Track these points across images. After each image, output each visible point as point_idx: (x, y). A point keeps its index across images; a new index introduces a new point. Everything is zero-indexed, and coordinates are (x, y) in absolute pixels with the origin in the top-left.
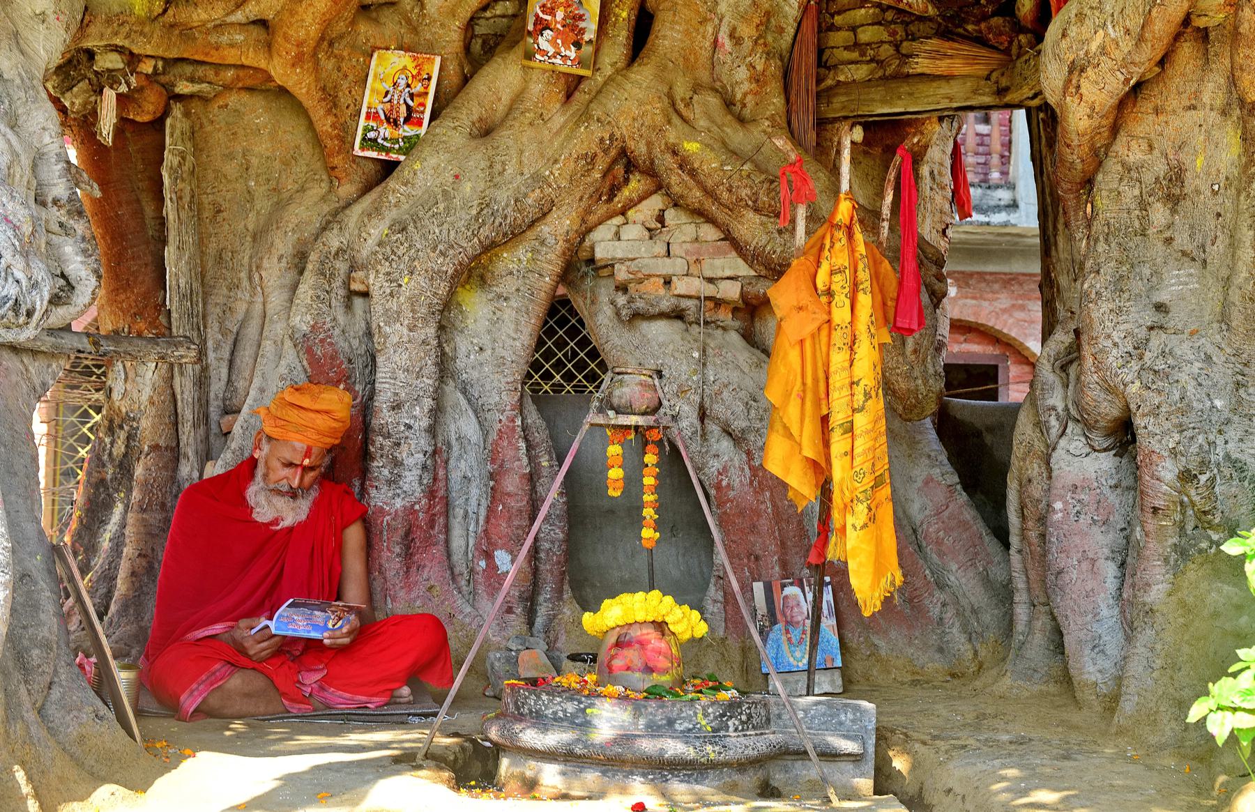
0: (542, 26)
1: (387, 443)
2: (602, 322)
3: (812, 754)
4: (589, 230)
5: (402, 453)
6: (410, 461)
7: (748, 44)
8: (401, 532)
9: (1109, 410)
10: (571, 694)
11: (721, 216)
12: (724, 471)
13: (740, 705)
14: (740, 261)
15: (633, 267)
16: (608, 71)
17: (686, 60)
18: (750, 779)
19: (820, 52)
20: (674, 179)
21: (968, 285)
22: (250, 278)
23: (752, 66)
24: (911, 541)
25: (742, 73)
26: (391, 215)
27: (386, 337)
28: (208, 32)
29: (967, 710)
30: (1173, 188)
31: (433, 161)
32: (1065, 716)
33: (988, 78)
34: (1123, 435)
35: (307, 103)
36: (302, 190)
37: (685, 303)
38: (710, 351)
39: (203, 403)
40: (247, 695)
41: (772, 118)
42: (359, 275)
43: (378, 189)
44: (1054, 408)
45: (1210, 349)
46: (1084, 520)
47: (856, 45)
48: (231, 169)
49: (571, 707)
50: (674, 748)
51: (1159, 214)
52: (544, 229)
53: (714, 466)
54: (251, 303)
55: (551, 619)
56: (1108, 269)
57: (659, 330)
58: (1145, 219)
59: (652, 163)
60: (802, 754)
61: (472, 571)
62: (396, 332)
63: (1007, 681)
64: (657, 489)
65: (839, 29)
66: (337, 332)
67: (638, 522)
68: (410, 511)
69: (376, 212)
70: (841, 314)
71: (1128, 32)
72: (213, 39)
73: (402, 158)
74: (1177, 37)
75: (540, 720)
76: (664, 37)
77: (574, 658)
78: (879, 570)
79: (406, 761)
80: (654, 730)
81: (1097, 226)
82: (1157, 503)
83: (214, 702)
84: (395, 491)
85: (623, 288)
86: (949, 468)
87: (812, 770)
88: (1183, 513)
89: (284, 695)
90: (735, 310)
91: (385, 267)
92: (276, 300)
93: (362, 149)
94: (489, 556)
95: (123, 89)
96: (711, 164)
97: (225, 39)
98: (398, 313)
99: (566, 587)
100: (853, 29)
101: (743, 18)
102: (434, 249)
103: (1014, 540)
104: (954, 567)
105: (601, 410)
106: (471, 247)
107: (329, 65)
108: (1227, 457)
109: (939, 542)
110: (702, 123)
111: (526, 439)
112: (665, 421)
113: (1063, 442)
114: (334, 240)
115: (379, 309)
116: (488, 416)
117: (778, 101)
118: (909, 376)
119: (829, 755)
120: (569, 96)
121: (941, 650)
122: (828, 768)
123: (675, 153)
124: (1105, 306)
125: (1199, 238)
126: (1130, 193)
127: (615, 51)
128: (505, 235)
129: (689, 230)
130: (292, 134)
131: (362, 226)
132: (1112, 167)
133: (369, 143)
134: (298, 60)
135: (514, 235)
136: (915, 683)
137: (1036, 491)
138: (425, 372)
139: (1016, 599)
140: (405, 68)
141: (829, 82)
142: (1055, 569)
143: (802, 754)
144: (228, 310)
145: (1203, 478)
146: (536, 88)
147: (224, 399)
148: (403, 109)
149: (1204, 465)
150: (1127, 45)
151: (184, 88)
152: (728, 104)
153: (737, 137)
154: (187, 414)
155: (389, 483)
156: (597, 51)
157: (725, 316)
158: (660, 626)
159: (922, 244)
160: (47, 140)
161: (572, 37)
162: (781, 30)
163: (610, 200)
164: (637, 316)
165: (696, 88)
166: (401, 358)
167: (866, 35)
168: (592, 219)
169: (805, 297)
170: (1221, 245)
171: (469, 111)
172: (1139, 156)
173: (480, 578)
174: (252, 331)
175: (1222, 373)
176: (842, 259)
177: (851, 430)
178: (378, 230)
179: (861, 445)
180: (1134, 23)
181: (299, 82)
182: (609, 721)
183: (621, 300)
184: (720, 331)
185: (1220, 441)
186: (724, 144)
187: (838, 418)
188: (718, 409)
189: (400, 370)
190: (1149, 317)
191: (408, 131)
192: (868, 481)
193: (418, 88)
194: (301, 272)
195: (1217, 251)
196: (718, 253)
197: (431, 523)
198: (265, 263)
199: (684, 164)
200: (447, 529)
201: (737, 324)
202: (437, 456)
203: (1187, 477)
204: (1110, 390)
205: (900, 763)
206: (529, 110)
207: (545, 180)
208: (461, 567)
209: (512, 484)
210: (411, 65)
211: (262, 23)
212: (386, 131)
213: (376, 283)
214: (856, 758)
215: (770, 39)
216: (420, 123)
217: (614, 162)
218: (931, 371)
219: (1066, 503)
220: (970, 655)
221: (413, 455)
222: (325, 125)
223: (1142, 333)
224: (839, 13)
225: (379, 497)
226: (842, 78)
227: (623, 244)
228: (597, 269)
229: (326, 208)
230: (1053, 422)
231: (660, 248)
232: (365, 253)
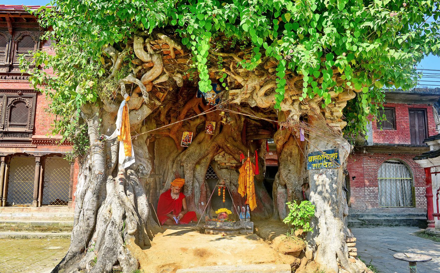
0: (207, 128)
2: (216, 169)
9: (283, 183)
11: (233, 155)
12: (233, 190)
18: (237, 232)
19: (246, 130)
24: (259, 200)
25: (235, 134)
26: (186, 155)
30: (291, 155)
34: (285, 186)
39: (160, 181)
46: (281, 197)
47: (251, 130)
50: (228, 228)
51: (289, 158)
52: (208, 157)
53: (232, 190)
57: (224, 170)
58: (287, 159)
60: (244, 229)
62: (188, 172)
67: (223, 199)
68: (189, 197)
69: (184, 154)
70: (248, 173)
74: (290, 136)
75: (210, 225)
77: (214, 217)
78: (253, 205)
79: (193, 230)
80: (225, 226)
84: (188, 194)
85: (219, 164)
87: (245, 231)
90: (235, 167)
92: (170, 167)
94: (200, 203)
96: (231, 148)
101: (236, 127)
106: (198, 160)
114: (179, 159)
117: (240, 138)
119: (248, 229)
126: (285, 155)
127: (217, 132)
129: (228, 156)
130: (172, 143)
132: (283, 152)
134: (174, 134)
135: (203, 158)
143: (244, 229)
144: (163, 168)
146: (207, 137)
149: (295, 191)
150: (283, 139)
151: (157, 137)
152: (233, 138)
153: (235, 144)
154: (158, 183)
157: (233, 168)
158: (226, 213)
159: (260, 158)
165: (229, 137)
166: (188, 175)
167: (253, 128)
169: (244, 171)
171: (197, 140)
174: (167, 171)
175: (297, 179)
176: (248, 165)
180: (284, 136)
181: (174, 137)
182: (219, 224)
187: (248, 186)
188: (233, 182)
190: (288, 171)
191: (189, 143)
194: (174, 163)
195: (296, 163)
196: (232, 159)
199: (227, 147)
203: (293, 192)
205: (257, 230)
209: (204, 193)
211: (169, 129)
214: (251, 229)
221: (190, 189)
222: (177, 142)
231: (224, 159)
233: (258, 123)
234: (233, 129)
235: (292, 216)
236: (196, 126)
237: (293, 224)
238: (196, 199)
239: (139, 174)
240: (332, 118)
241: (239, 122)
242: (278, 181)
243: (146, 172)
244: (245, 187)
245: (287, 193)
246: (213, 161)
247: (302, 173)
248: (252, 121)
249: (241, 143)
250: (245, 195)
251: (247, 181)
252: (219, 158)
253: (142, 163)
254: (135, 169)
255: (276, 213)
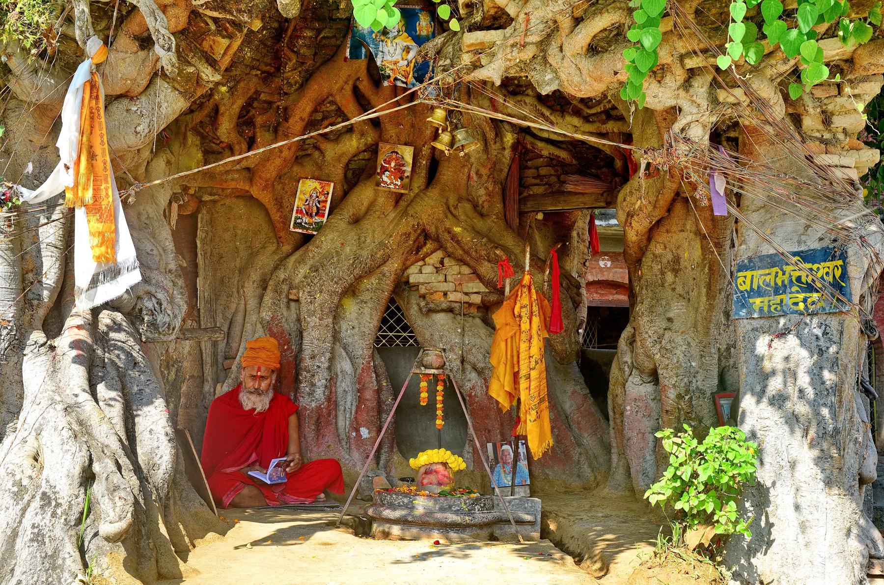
0: (384, 170)
1: (308, 375)
2: (413, 312)
3: (512, 521)
4: (407, 268)
5: (316, 380)
6: (319, 384)
7: (485, 178)
8: (315, 419)
9: (648, 365)
10: (405, 495)
11: (472, 263)
13: (480, 499)
14: (481, 284)
15: (428, 288)
16: (416, 191)
17: (455, 185)
18: (485, 532)
19: (521, 179)
20: (449, 245)
21: (618, 260)
22: (238, 292)
23: (487, 188)
24: (560, 423)
25: (482, 191)
26: (310, 262)
27: (308, 323)
28: (222, 174)
29: (586, 504)
30: (675, 266)
31: (331, 236)
32: (630, 506)
33: (602, 195)
34: (654, 376)
35: (268, 206)
36: (264, 247)
37: (454, 305)
38: (466, 329)
39: (215, 354)
40: (251, 497)
41: (497, 215)
42: (294, 291)
43: (303, 249)
44: (626, 362)
45: (690, 340)
46: (640, 415)
47: (538, 176)
48: (227, 236)
49: (406, 500)
50: (452, 517)
51: (670, 277)
52: (385, 269)
53: (468, 385)
54: (238, 304)
55: (388, 461)
56: (647, 302)
57: (441, 318)
58: (663, 280)
59: (438, 236)
61: (348, 438)
62: (313, 321)
63: (606, 490)
64: (443, 402)
65: (530, 168)
66: (284, 320)
67: (434, 417)
68: (319, 408)
69: (302, 261)
70: (525, 326)
71: (650, 202)
72: (224, 177)
73: (315, 233)
75: (392, 506)
76: (444, 175)
77: (403, 480)
78: (541, 439)
79: (331, 525)
80: (442, 510)
81: (643, 282)
82: (668, 408)
83: (237, 500)
85: (423, 297)
86: (584, 386)
87: (513, 529)
88: (679, 413)
89: (266, 497)
91: (308, 289)
92: (252, 303)
93: (294, 228)
94: (357, 430)
95: (182, 202)
96: (467, 238)
97: (230, 177)
98: (314, 312)
99: (395, 445)
100: (537, 168)
101: (483, 165)
102: (332, 281)
103: (611, 423)
104: (586, 435)
105: (418, 367)
106: (350, 279)
107: (279, 187)
108: (697, 388)
109: (579, 423)
110: (462, 217)
111: (375, 373)
112: (447, 372)
113: (630, 379)
114: (282, 275)
115: (305, 309)
116: (357, 361)
117: (499, 206)
118: (562, 343)
119: (520, 522)
120: (397, 202)
121: (579, 476)
122: (519, 528)
123: (449, 232)
124: (646, 319)
125: (686, 288)
126: (657, 268)
127: (419, 181)
128: (366, 272)
129: (456, 268)
130: (259, 219)
131: (295, 268)
132: (649, 255)
133: (298, 225)
134: (265, 188)
136: (566, 492)
137: (619, 400)
138: (327, 340)
139: (613, 451)
140: (316, 188)
141: (525, 194)
142: (627, 438)
143: (508, 522)
145: (687, 398)
146: (381, 200)
147: (225, 352)
148: (315, 208)
149: (687, 391)
150: (650, 208)
151: (207, 198)
152: (475, 206)
153: (480, 224)
154: (208, 359)
155: (309, 394)
156: (411, 180)
157: (473, 311)
158: (445, 464)
159: (568, 277)
160: (167, 244)
161: (399, 175)
162: (501, 170)
163: (417, 253)
164: (431, 311)
165: (460, 199)
166: (315, 334)
167: (543, 171)
168: (408, 263)
169: (509, 319)
170: (695, 293)
172: (660, 251)
173: (352, 441)
174: (239, 318)
175: (695, 351)
176: (525, 301)
177: (529, 378)
178: (303, 270)
179: (534, 384)
180: (652, 199)
181: (265, 198)
182: (421, 505)
183: (423, 304)
184: (471, 319)
185: (694, 381)
186: (473, 227)
187: (523, 373)
188: (470, 358)
189: (315, 339)
190: (664, 324)
191: (317, 219)
192: (536, 401)
193: (322, 198)
194: (265, 289)
195: (693, 295)
196: (470, 280)
197: (329, 414)
198: (246, 285)
199: (454, 237)
200: (336, 416)
201: (480, 314)
202: (332, 382)
203: (680, 397)
204: (648, 356)
205: (552, 527)
206: (377, 211)
207: (386, 245)
208: (343, 436)
209: (369, 395)
210: (319, 187)
211: (248, 169)
212: (306, 219)
213: (303, 296)
215: (496, 175)
216: (323, 216)
217: (419, 235)
218: (573, 340)
219: (631, 407)
220: (593, 478)
221: (320, 381)
222: (276, 216)
223: (661, 331)
224: (530, 160)
225: (304, 401)
226: (531, 193)
227: (423, 275)
228: (410, 287)
229: (276, 257)
230: (626, 369)
232: (297, 281)
233: (563, 155)
234: (473, 174)
235: (675, 477)
236: (345, 160)
237: (678, 506)
238: (341, 418)
239: (143, 328)
240: (827, 136)
241: (494, 148)
242: (628, 358)
243: (167, 319)
244: (516, 376)
245: (658, 398)
246: (402, 285)
247: (714, 331)
248: (540, 145)
249: (502, 223)
250: (515, 403)
251: (519, 358)
252: (422, 275)
253: (152, 289)
254: (127, 310)
255: (621, 470)
